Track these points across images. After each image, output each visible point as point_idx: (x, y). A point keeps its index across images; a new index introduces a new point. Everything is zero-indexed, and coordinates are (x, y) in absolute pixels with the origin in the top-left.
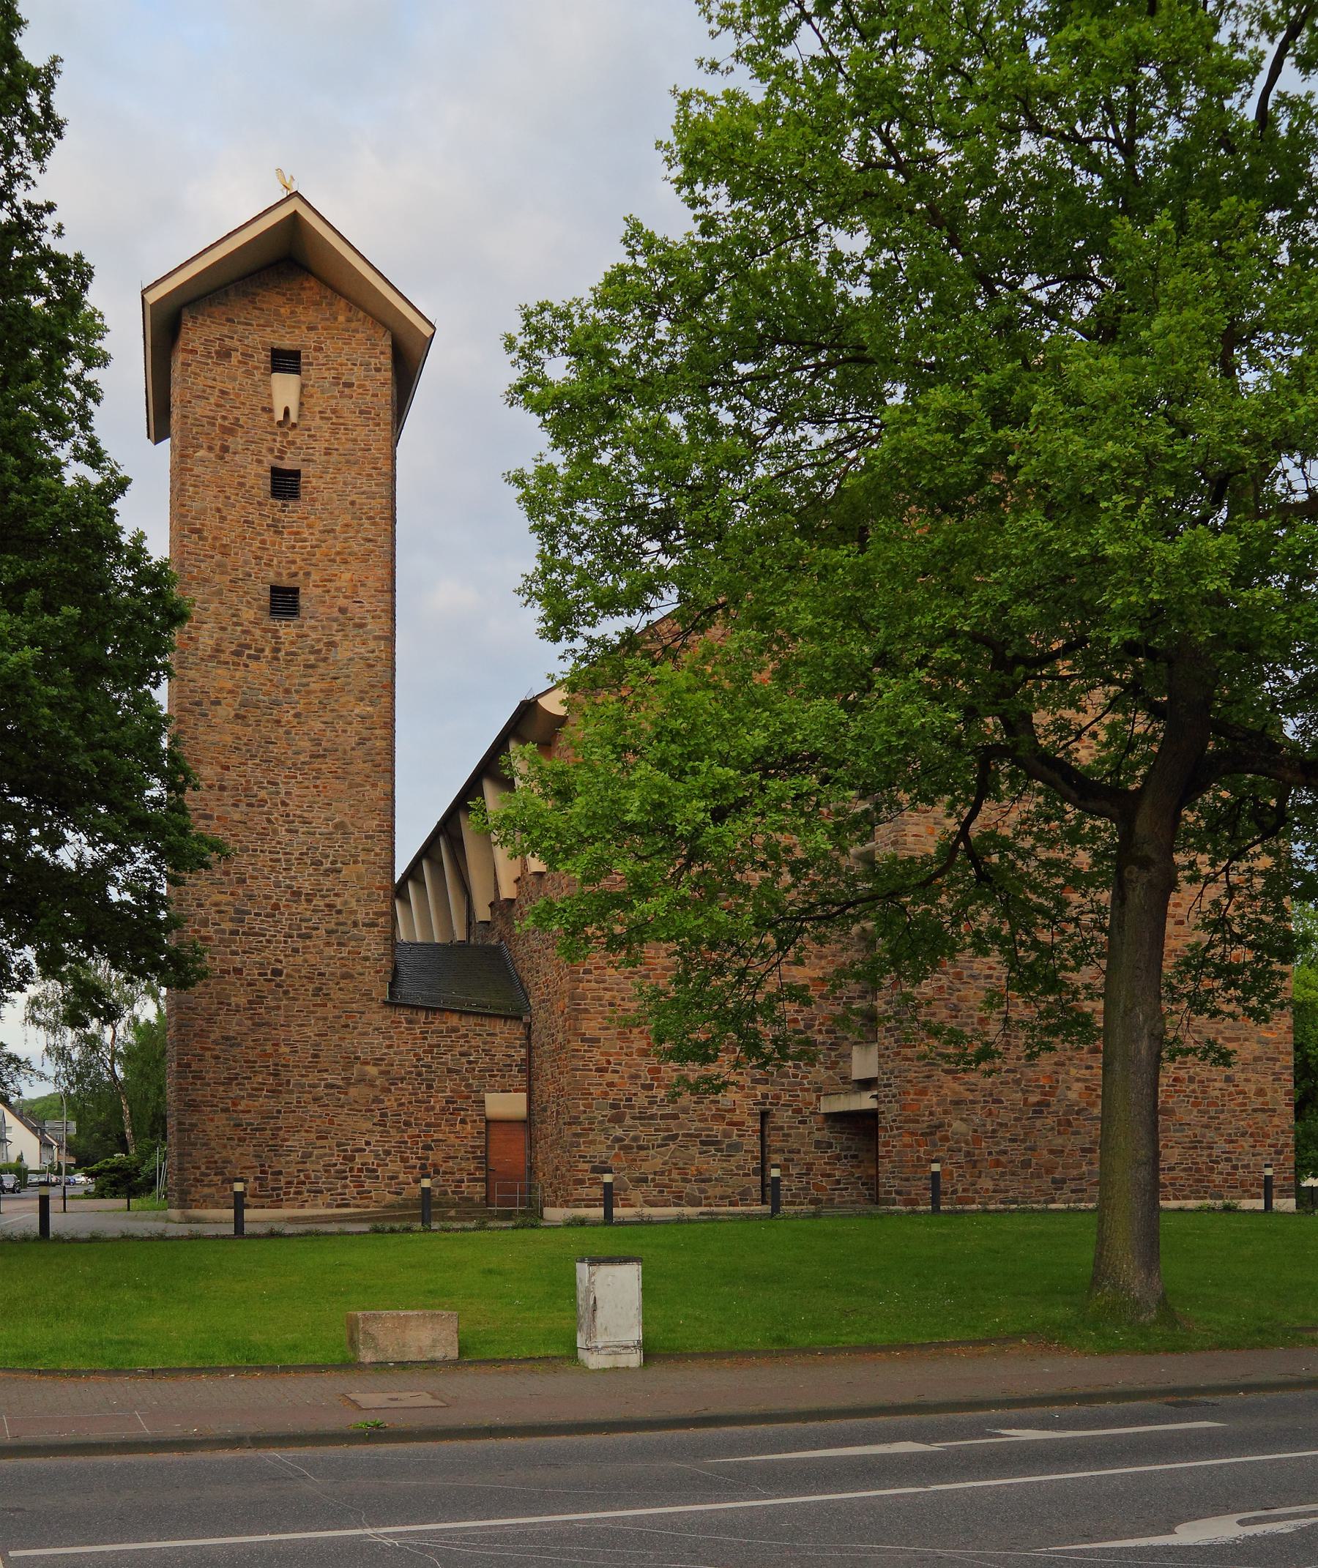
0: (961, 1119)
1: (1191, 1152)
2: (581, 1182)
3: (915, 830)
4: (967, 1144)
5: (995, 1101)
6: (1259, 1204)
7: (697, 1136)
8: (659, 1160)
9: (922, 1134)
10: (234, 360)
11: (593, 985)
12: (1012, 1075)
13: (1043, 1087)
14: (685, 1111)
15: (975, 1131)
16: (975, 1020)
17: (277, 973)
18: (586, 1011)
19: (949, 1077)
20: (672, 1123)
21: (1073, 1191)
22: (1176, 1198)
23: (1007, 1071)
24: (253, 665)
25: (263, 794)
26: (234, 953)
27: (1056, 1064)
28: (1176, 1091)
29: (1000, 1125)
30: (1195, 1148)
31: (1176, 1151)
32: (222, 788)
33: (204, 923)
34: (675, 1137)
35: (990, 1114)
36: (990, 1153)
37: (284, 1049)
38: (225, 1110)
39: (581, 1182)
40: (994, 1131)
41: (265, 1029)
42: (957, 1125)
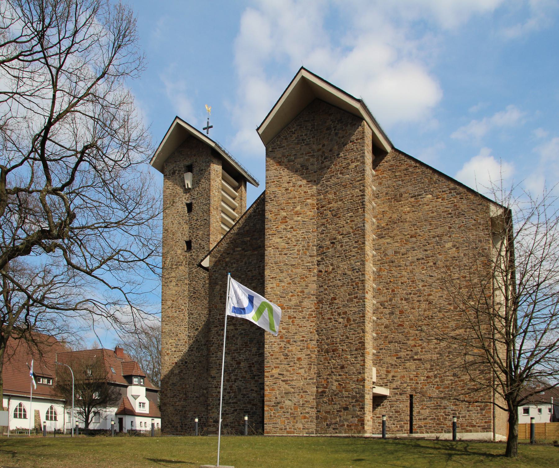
0: (289, 400)
1: (435, 411)
2: (210, 426)
3: (271, 286)
4: (291, 409)
5: (304, 392)
6: (449, 436)
7: (243, 409)
8: (232, 418)
9: (273, 406)
10: (176, 174)
11: (214, 358)
12: (312, 381)
13: (323, 385)
14: (239, 400)
15: (295, 404)
16: (295, 359)
17: (186, 362)
18: (212, 367)
19: (284, 383)
20: (236, 405)
21: (334, 429)
22: (427, 432)
23: (310, 379)
24: (180, 267)
25: (183, 307)
26: (175, 358)
27: (328, 375)
28: (428, 383)
29: (306, 401)
30: (437, 409)
31: (428, 410)
32: (172, 307)
33: (168, 349)
34: (236, 410)
35: (302, 397)
36: (301, 413)
37: (188, 386)
38: (173, 405)
39: (210, 426)
40: (303, 404)
41: (183, 380)
42: (288, 403)
